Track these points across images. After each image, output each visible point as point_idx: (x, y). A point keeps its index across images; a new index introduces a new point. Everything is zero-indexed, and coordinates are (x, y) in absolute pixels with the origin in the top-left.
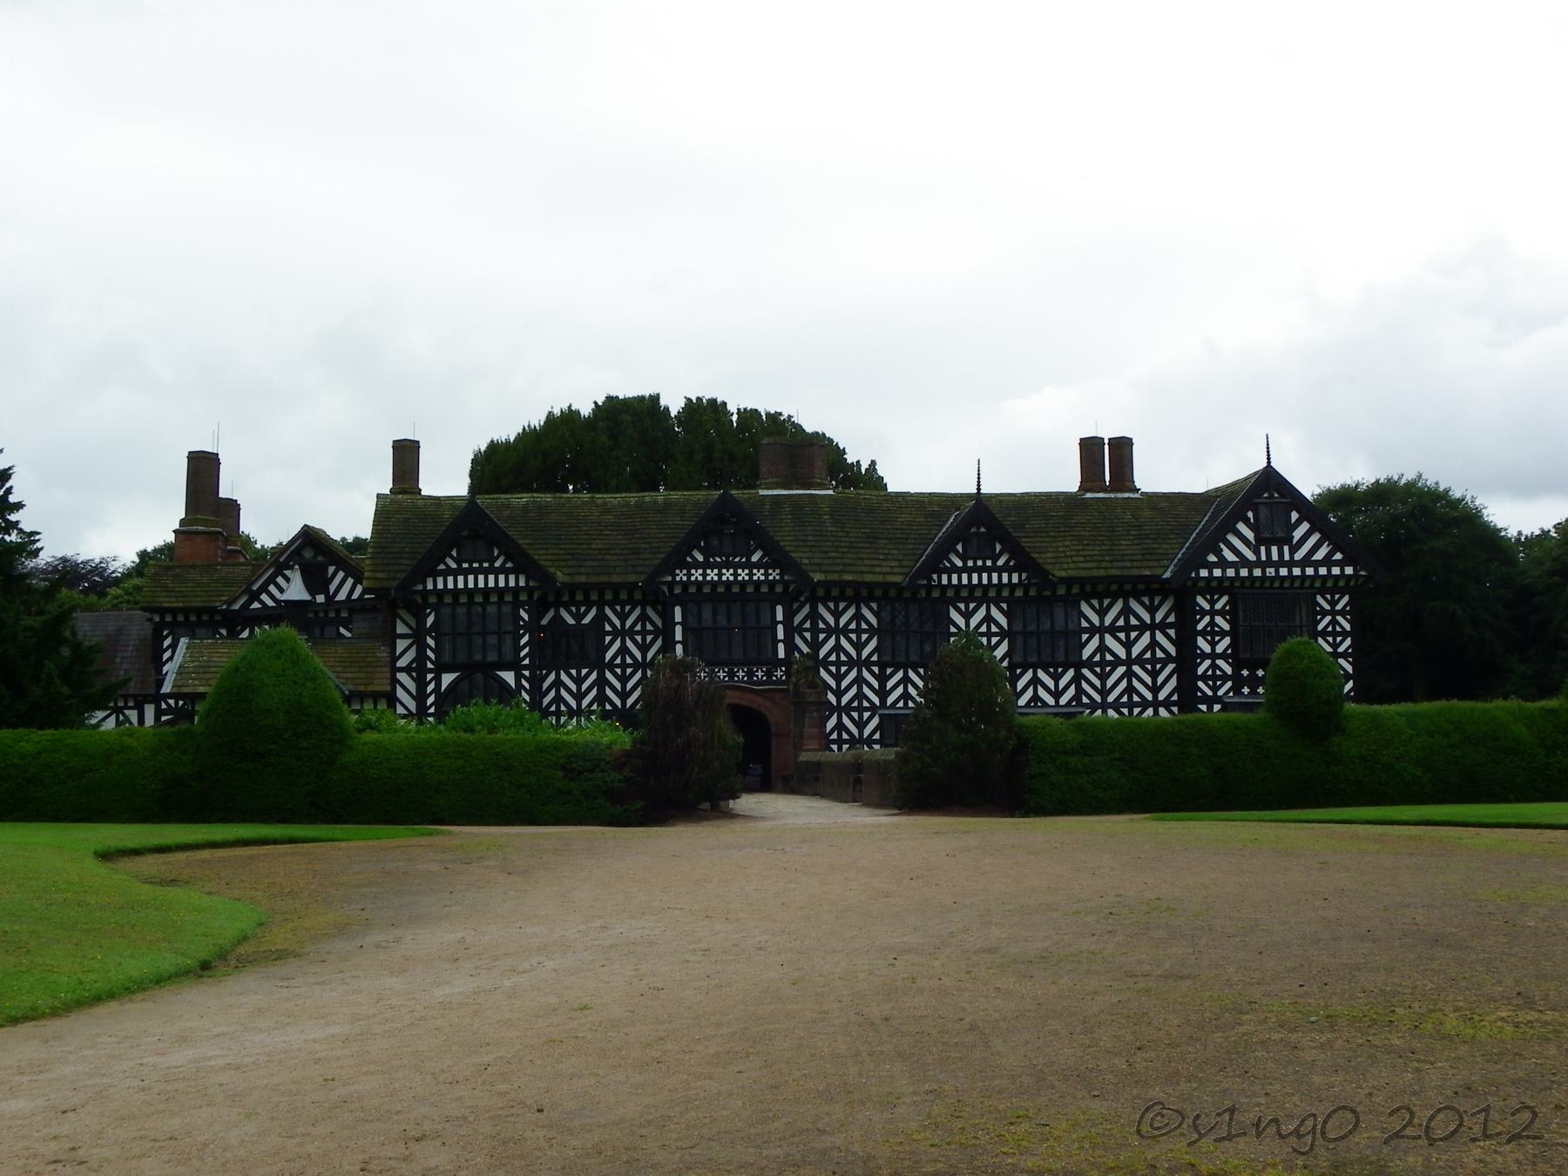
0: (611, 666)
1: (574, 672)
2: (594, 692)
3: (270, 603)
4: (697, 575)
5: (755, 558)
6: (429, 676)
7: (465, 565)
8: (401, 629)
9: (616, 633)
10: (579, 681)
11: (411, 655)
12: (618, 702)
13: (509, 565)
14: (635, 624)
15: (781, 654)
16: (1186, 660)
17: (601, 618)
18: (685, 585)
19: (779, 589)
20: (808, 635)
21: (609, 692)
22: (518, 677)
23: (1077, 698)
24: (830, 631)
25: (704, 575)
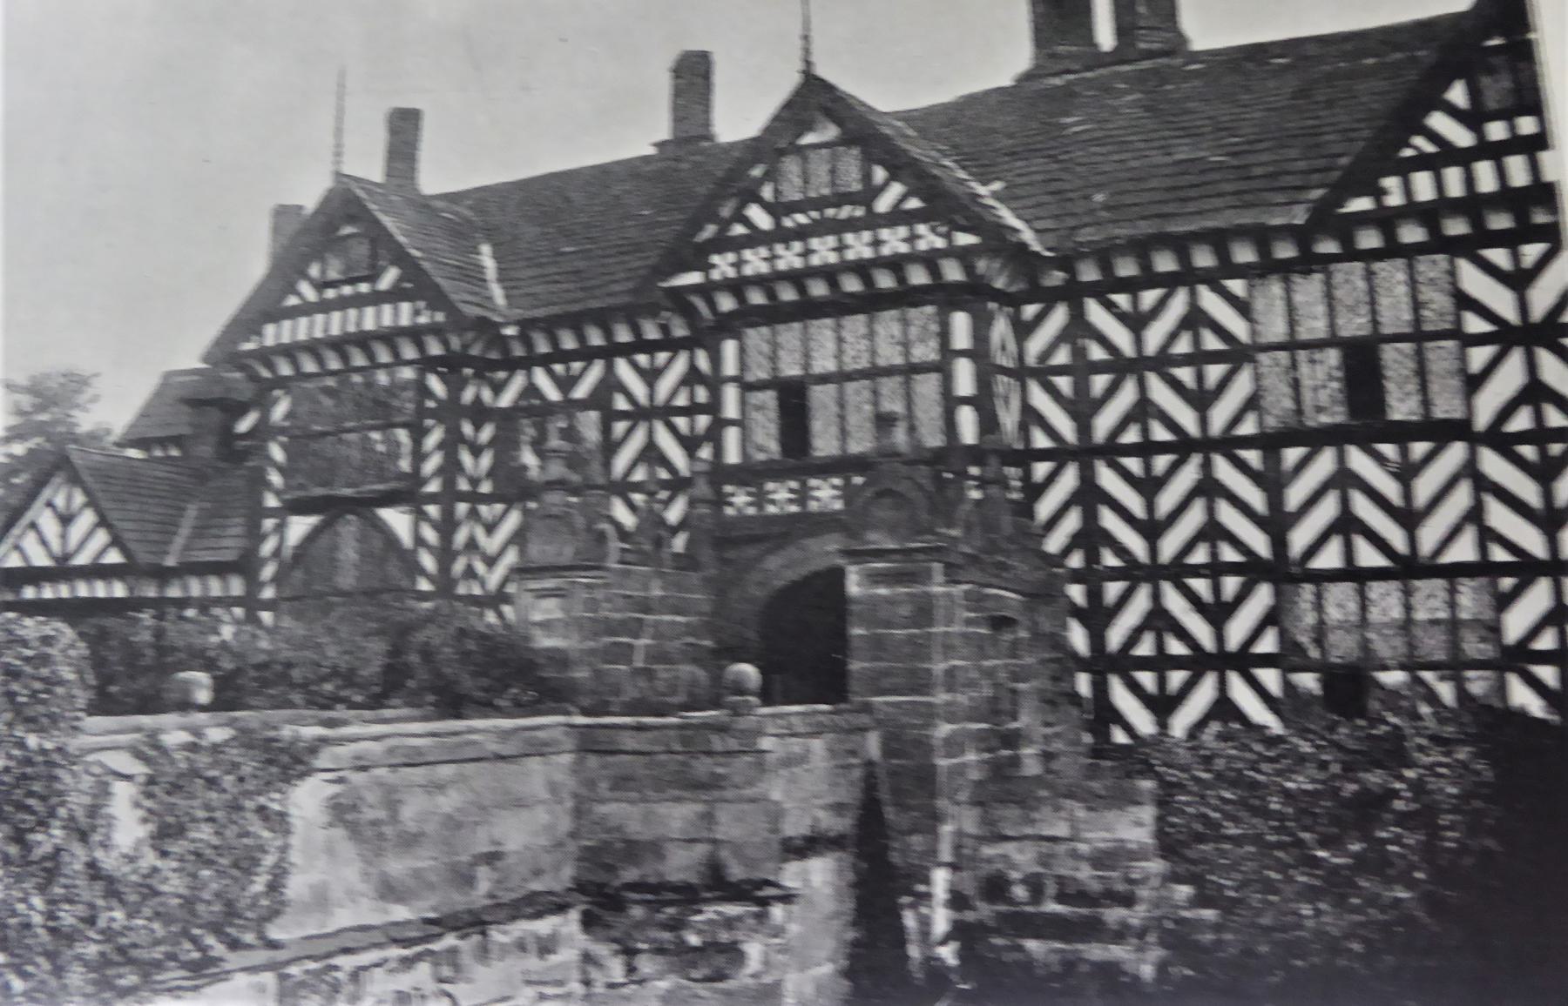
24: (1120, 367)
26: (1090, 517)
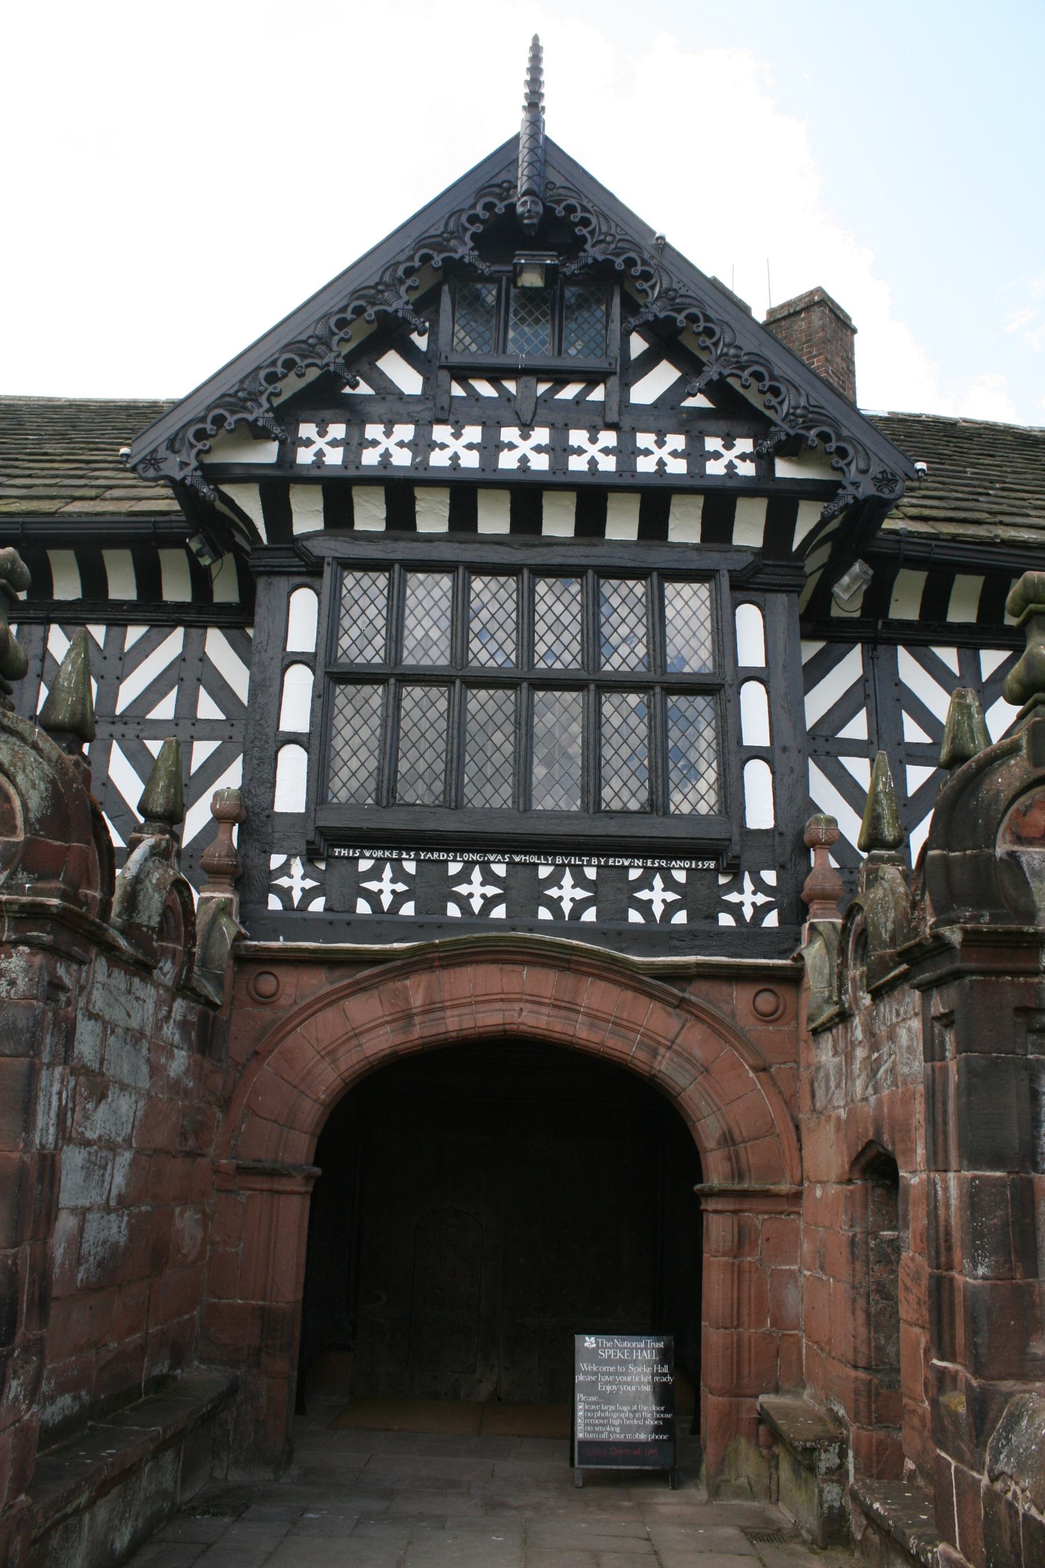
4: (390, 446)
5: (648, 390)
15: (760, 812)
18: (338, 493)
19: (749, 531)
20: (859, 769)
25: (422, 445)
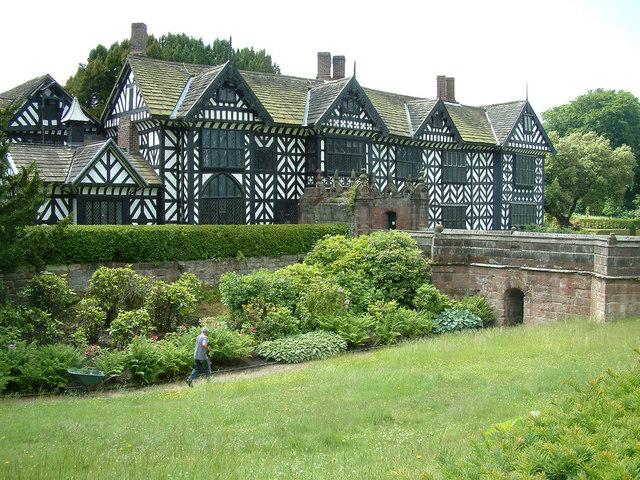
0: (280, 173)
1: (262, 176)
2: (272, 189)
3: (24, 124)
5: (362, 117)
6: (196, 175)
7: (221, 104)
8: (168, 143)
9: (284, 154)
10: (264, 181)
11: (173, 160)
12: (283, 195)
13: (245, 107)
14: (292, 149)
16: (498, 183)
17: (275, 144)
21: (279, 188)
22: (244, 177)
23: (463, 199)
26: (275, 188)
